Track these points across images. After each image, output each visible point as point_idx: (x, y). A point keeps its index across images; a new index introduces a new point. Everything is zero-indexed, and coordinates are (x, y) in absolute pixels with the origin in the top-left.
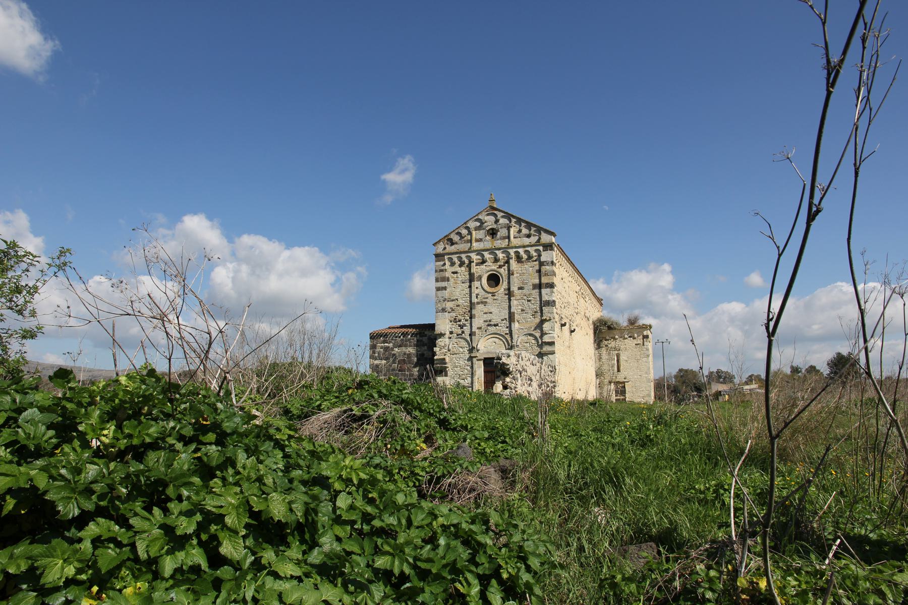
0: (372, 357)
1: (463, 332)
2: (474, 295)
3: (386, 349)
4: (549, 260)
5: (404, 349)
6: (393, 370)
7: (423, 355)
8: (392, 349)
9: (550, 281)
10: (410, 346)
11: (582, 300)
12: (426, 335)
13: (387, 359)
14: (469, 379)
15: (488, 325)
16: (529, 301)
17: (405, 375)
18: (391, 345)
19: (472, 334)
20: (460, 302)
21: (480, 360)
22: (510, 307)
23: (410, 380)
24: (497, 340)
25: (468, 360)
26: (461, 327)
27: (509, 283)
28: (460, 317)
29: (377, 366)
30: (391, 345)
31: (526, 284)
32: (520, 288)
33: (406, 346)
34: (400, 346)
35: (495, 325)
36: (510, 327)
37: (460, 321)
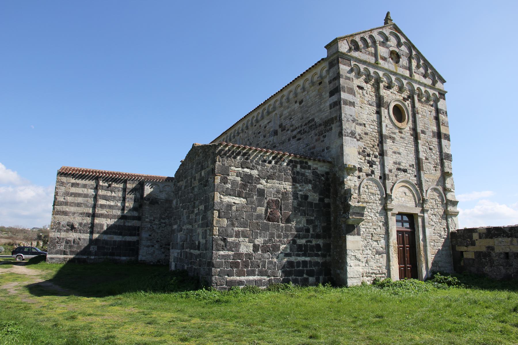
3: (247, 179)
6: (259, 217)
7: (306, 197)
12: (309, 168)
14: (383, 242)
15: (399, 169)
18: (255, 173)
19: (384, 177)
20: (368, 129)
21: (393, 215)
22: (417, 151)
23: (287, 236)
24: (406, 190)
25: (380, 214)
26: (371, 164)
27: (415, 122)
28: (368, 150)
29: (229, 206)
30: (255, 173)
33: (279, 178)
35: (405, 171)
36: (418, 176)
37: (369, 155)
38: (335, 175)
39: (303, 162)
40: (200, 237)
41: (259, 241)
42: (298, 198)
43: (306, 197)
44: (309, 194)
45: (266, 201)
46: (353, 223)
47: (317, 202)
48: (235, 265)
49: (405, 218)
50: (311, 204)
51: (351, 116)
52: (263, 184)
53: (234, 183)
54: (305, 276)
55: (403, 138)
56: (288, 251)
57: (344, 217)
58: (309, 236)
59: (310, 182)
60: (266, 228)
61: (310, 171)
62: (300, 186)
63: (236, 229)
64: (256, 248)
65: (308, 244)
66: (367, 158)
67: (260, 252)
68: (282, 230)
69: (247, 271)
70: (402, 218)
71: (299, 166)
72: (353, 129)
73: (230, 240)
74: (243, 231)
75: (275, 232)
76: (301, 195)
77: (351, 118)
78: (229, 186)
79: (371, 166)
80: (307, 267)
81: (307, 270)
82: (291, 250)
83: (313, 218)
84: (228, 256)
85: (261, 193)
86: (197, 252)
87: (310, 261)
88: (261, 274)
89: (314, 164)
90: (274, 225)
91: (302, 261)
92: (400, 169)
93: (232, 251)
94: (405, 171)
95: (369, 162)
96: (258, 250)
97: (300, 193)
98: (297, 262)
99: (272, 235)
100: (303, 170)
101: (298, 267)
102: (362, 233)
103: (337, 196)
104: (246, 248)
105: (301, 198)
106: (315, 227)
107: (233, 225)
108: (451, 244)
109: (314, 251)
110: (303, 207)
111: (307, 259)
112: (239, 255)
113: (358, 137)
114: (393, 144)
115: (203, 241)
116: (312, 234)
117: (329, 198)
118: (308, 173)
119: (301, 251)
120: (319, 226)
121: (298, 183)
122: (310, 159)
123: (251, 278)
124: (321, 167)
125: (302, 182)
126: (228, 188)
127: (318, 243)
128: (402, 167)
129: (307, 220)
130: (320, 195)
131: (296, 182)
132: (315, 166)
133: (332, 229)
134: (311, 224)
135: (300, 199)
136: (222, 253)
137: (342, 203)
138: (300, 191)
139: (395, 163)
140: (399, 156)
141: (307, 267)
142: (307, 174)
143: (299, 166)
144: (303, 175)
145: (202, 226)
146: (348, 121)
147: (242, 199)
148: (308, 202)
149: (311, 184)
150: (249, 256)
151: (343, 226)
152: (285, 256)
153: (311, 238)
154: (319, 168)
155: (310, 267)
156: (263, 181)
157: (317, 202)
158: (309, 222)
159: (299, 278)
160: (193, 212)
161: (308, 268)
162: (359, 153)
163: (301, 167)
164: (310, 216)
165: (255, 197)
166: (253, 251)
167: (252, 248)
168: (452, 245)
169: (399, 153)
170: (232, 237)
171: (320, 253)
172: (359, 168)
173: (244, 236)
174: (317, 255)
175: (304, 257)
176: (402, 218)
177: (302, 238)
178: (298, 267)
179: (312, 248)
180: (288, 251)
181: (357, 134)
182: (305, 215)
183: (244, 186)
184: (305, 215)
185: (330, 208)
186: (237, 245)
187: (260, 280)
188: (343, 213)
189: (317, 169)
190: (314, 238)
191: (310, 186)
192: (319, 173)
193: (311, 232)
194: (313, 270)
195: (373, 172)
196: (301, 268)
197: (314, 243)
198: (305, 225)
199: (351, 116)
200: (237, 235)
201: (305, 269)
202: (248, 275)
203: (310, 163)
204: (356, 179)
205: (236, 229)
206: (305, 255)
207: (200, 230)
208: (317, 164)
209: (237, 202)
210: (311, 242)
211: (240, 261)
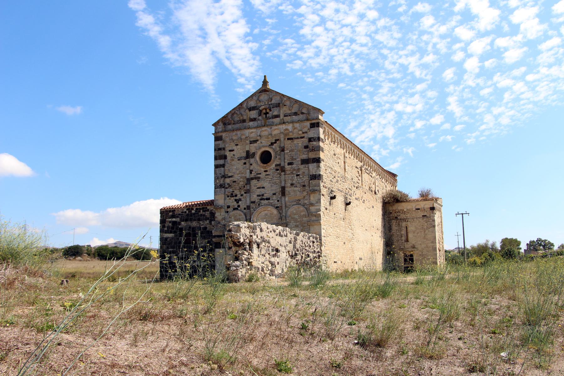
1: (239, 206)
3: (174, 223)
4: (316, 136)
5: (189, 223)
7: (205, 228)
8: (180, 224)
9: (317, 156)
10: (195, 220)
11: (365, 176)
12: (208, 210)
13: (175, 232)
15: (261, 199)
16: (297, 175)
29: (166, 239)
31: (295, 159)
32: (289, 164)
33: (191, 220)
34: (186, 220)
43: (205, 228)
53: (168, 227)
59: (208, 219)
66: (235, 198)
71: (201, 211)
72: (222, 182)
78: (166, 229)
85: (181, 229)
107: (168, 248)
113: (227, 186)
118: (207, 214)
122: (208, 205)
128: (264, 197)
139: (258, 196)
143: (201, 211)
144: (204, 215)
156: (183, 223)
169: (263, 188)
173: (173, 253)
183: (172, 228)
203: (208, 208)
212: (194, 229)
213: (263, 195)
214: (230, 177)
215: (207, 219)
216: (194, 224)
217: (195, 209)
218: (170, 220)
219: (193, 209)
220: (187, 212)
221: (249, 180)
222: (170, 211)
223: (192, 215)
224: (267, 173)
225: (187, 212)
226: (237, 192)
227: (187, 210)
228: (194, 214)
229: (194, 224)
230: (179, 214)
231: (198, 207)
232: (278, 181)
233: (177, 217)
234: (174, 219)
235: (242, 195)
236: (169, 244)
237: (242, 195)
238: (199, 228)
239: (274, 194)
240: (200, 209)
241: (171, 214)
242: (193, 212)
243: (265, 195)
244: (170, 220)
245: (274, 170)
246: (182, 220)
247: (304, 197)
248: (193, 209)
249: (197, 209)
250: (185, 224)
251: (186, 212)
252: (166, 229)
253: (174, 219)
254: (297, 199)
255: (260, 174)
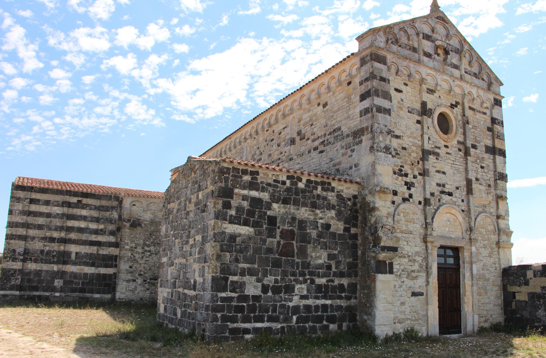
0: (220, 216)
2: (426, 137)
3: (256, 202)
5: (292, 209)
6: (269, 251)
7: (327, 226)
10: (305, 205)
12: (333, 190)
13: (256, 225)
15: (442, 192)
17: (293, 264)
26: (409, 185)
29: (233, 237)
33: (296, 203)
34: (286, 202)
35: (450, 194)
37: (406, 175)
38: (364, 199)
39: (325, 182)
40: (197, 274)
41: (270, 280)
42: (317, 227)
43: (327, 226)
44: (332, 222)
45: (278, 231)
46: (385, 259)
47: (342, 232)
48: (240, 309)
49: (450, 252)
50: (334, 235)
51: (386, 126)
52: (277, 209)
53: (239, 209)
54: (325, 323)
55: (449, 154)
56: (305, 292)
57: (374, 252)
58: (330, 273)
59: (333, 207)
60: (277, 264)
61: (333, 194)
62: (321, 212)
63: (241, 265)
64: (265, 289)
65: (330, 283)
66: (405, 179)
67: (270, 294)
68: (298, 268)
69: (255, 316)
70: (445, 252)
71: (320, 188)
72: (388, 142)
73: (232, 278)
74: (249, 269)
75: (290, 269)
76: (322, 224)
77: (386, 129)
78: (233, 212)
79: (409, 189)
80: (327, 312)
81: (327, 316)
82: (308, 291)
83: (336, 252)
84: (231, 299)
85: (272, 221)
86: (192, 293)
87: (331, 305)
88: (271, 319)
89: (339, 185)
90: (289, 260)
91: (322, 305)
92: (445, 192)
93: (236, 292)
94: (450, 194)
95: (406, 183)
96: (268, 292)
97: (321, 221)
98: (315, 306)
99: (285, 274)
100: (325, 193)
101: (316, 311)
102: (395, 270)
103: (366, 225)
104: (252, 289)
105: (322, 227)
106: (338, 263)
107: (237, 260)
108: (502, 283)
109: (336, 293)
110: (324, 238)
111: (328, 302)
112: (244, 298)
114: (436, 161)
115: (200, 280)
116: (334, 272)
117: (357, 228)
118: (331, 197)
119: (321, 292)
120: (343, 262)
121: (319, 209)
123: (259, 325)
124: (348, 188)
125: (323, 208)
126: (231, 216)
127: (342, 282)
128: (447, 190)
129: (329, 255)
130: (345, 223)
131: (316, 208)
132: (340, 188)
133: (360, 265)
134: (333, 259)
135: (320, 229)
136: (223, 295)
137: (372, 234)
138: (321, 219)
139: (438, 185)
140: (443, 176)
141: (327, 312)
142: (330, 198)
143: (320, 188)
144: (325, 198)
145: (199, 261)
146: (381, 132)
147: (247, 228)
148: (330, 232)
149: (334, 209)
150: (256, 298)
151: (372, 262)
152: (300, 298)
153: (334, 276)
154: (345, 191)
155: (331, 312)
156: (275, 206)
157: (342, 232)
158: (331, 257)
159: (318, 325)
160: (187, 242)
161: (329, 314)
162: (395, 173)
163: (322, 189)
164: (333, 249)
165: (265, 226)
166: (262, 292)
167: (260, 289)
168: (503, 284)
169: (444, 173)
170: (235, 275)
171: (343, 295)
172: (393, 191)
174: (340, 298)
175: (323, 300)
176: (445, 252)
177: (322, 277)
178: (316, 312)
179: (334, 288)
180: (305, 292)
181: (392, 149)
182: (326, 249)
183: (251, 213)
184: (326, 249)
185: (357, 239)
186: (242, 285)
187: (270, 328)
188: (373, 247)
189: (342, 191)
190: (337, 277)
191: (333, 213)
192: (345, 196)
193: (334, 269)
194: (335, 315)
195: (411, 196)
196: (320, 313)
197: (337, 282)
198: (326, 261)
199: (386, 126)
200: (243, 274)
201: (325, 314)
202: (256, 321)
203: (334, 184)
204: (389, 204)
205: (241, 265)
206: (325, 297)
207: (196, 266)
208: (342, 185)
209: (242, 232)
210: (333, 281)
211: (245, 304)
212: (302, 224)
213: (444, 186)
214: (397, 137)
215: (330, 207)
216: (304, 213)
217: (304, 181)
218: (245, 192)
219: (300, 180)
220: (288, 183)
221: (425, 154)
222: (245, 172)
223: (298, 191)
224: (449, 150)
225: (288, 183)
226: (407, 169)
227: (288, 177)
228: (303, 191)
229: (304, 213)
230: (269, 185)
231: (313, 178)
232: (462, 169)
233: (263, 190)
234: (254, 194)
235: (415, 177)
236: (241, 251)
237: (415, 177)
238: (315, 224)
239: (457, 188)
240: (317, 183)
241: (247, 178)
242: (301, 185)
243: (446, 186)
244: (245, 192)
245: (457, 149)
246: (275, 199)
247: (490, 202)
248: (300, 180)
249: (309, 181)
250: (283, 211)
251: (284, 183)
252: (233, 212)
253: (254, 194)
254: (483, 203)
255: (439, 148)
